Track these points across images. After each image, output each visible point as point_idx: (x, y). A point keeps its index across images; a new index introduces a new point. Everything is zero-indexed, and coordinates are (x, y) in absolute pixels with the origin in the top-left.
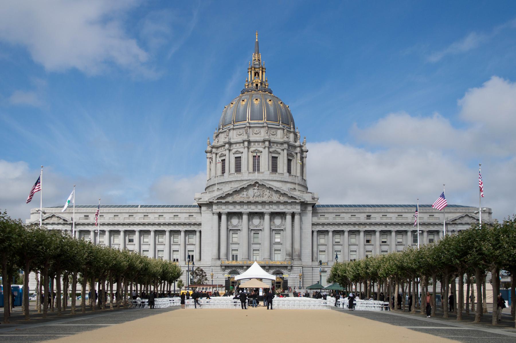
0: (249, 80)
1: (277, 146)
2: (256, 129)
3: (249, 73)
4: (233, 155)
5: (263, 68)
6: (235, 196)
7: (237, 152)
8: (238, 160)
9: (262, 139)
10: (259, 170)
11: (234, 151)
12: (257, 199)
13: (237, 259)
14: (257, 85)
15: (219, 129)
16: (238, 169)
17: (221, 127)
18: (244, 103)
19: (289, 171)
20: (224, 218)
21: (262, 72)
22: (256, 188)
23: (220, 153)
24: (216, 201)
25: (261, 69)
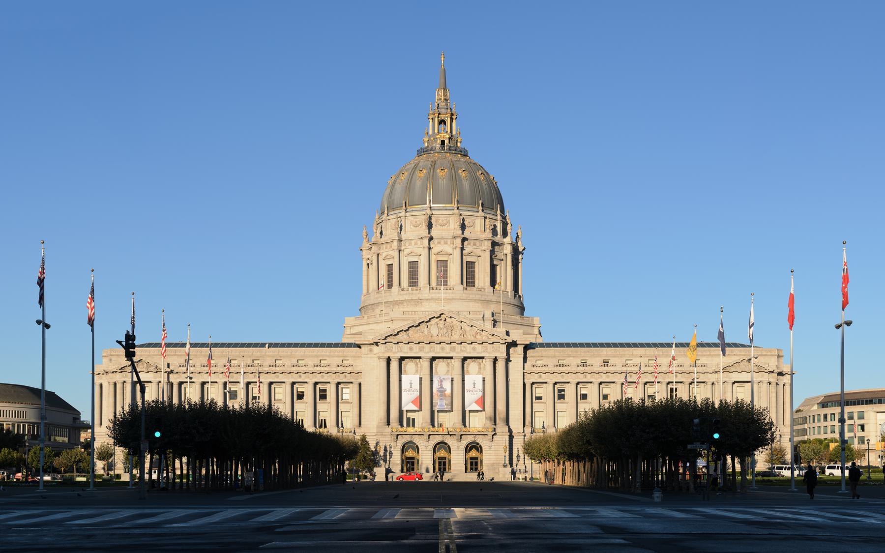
0: (431, 132)
1: (475, 245)
2: (442, 218)
3: (431, 121)
4: (405, 258)
5: (452, 115)
6: (411, 331)
7: (408, 255)
8: (413, 266)
9: (451, 234)
10: (446, 284)
11: (406, 252)
12: (443, 339)
13: (413, 425)
14: (443, 142)
15: (383, 213)
16: (413, 281)
17: (386, 212)
18: (422, 175)
19: (493, 283)
20: (394, 365)
21: (452, 119)
22: (442, 322)
23: (384, 255)
24: (384, 341)
25: (449, 115)
